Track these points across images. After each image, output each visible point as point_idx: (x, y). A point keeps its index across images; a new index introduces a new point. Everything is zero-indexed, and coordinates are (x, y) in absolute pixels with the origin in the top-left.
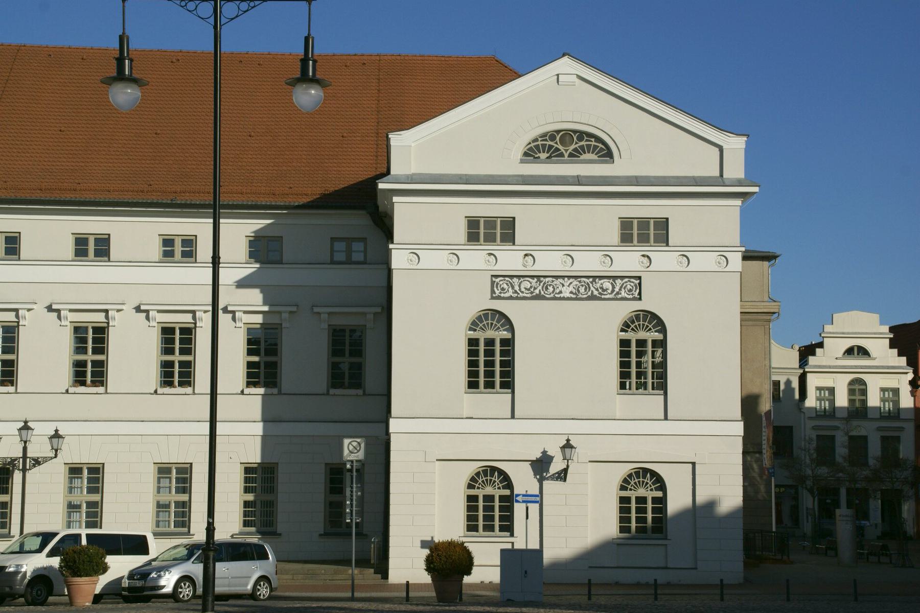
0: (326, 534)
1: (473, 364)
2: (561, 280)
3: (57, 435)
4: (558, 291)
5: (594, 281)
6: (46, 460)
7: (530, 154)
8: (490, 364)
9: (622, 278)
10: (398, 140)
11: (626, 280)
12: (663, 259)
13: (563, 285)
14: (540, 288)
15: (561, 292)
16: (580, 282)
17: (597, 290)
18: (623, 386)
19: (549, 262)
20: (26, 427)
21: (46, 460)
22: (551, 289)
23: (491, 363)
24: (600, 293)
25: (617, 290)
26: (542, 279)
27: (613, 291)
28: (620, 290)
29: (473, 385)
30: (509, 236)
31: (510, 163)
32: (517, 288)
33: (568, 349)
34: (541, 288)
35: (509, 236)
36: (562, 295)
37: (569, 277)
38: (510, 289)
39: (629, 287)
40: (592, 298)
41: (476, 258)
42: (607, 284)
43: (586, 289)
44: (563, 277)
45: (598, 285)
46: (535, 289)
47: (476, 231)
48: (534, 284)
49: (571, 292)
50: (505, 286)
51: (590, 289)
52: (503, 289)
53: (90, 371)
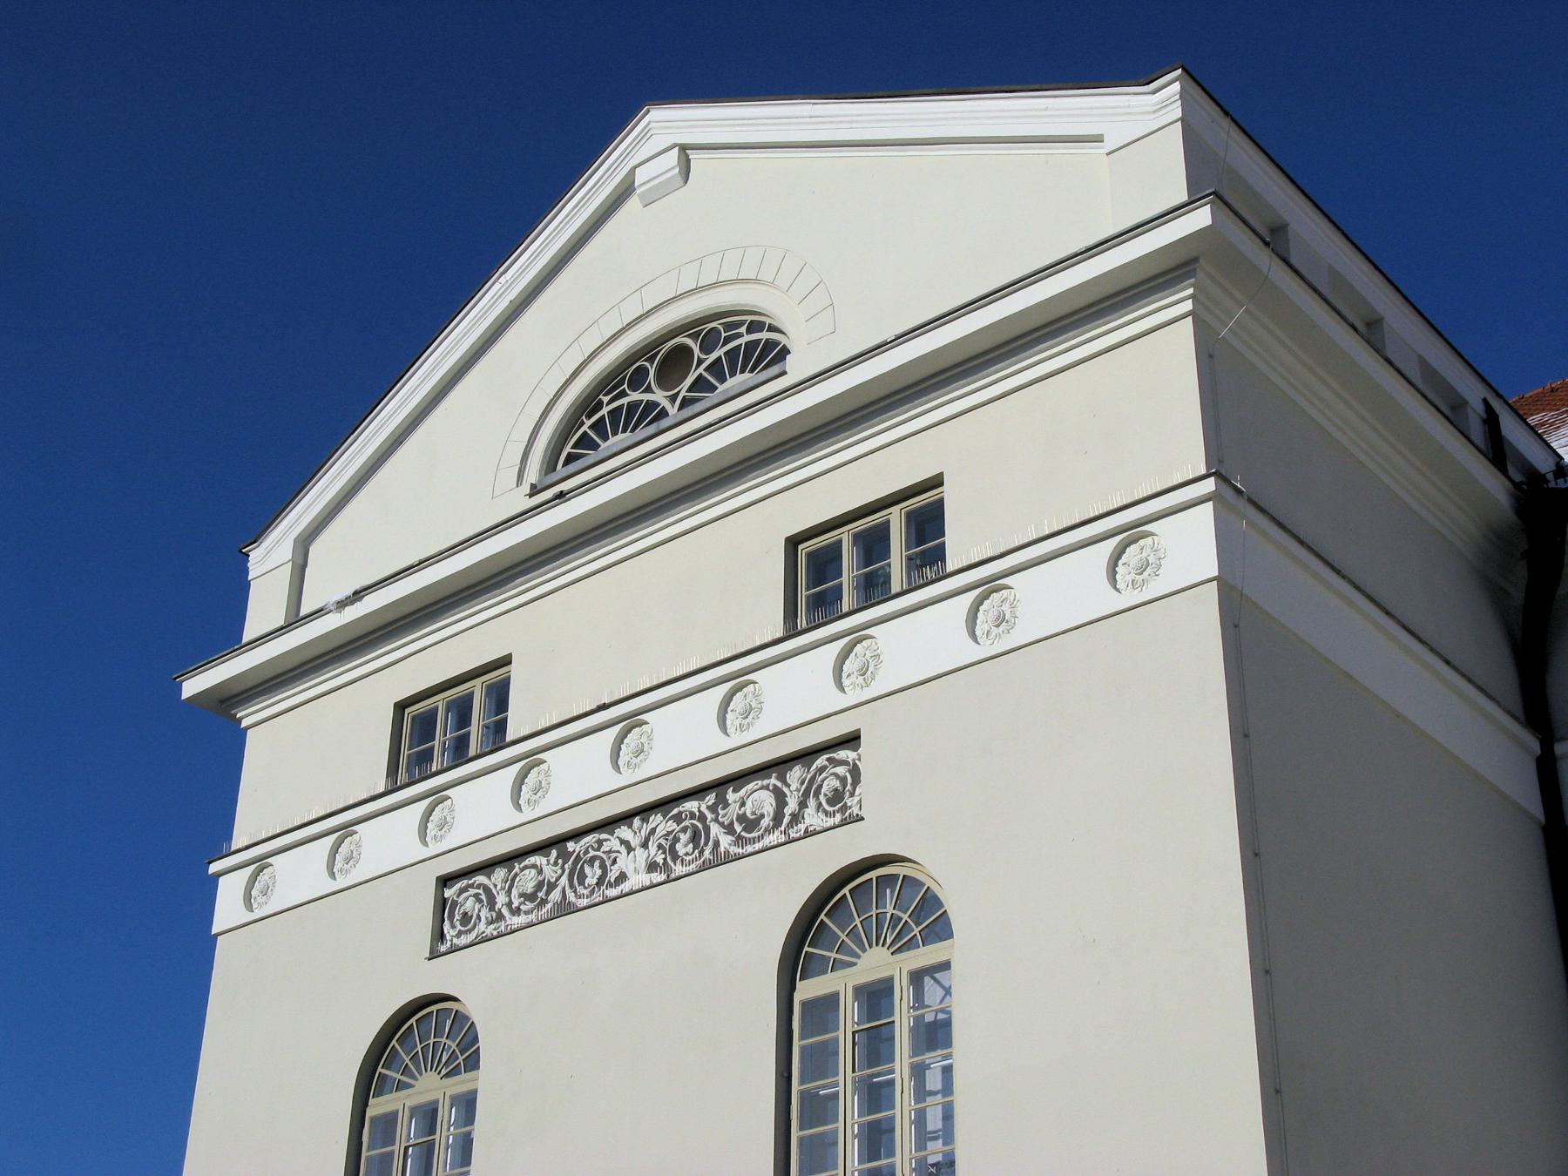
2: (624, 832)
4: (613, 875)
5: (722, 801)
9: (804, 756)
11: (821, 761)
12: (916, 637)
13: (630, 849)
14: (564, 880)
15: (622, 877)
16: (678, 819)
17: (729, 829)
22: (592, 874)
24: (739, 841)
25: (792, 805)
26: (571, 846)
27: (778, 818)
28: (803, 804)
32: (501, 899)
36: (625, 887)
37: (645, 811)
38: (484, 913)
39: (830, 784)
43: (695, 838)
44: (625, 818)
45: (733, 810)
46: (552, 886)
48: (550, 873)
49: (652, 867)
50: (469, 905)
52: (466, 918)
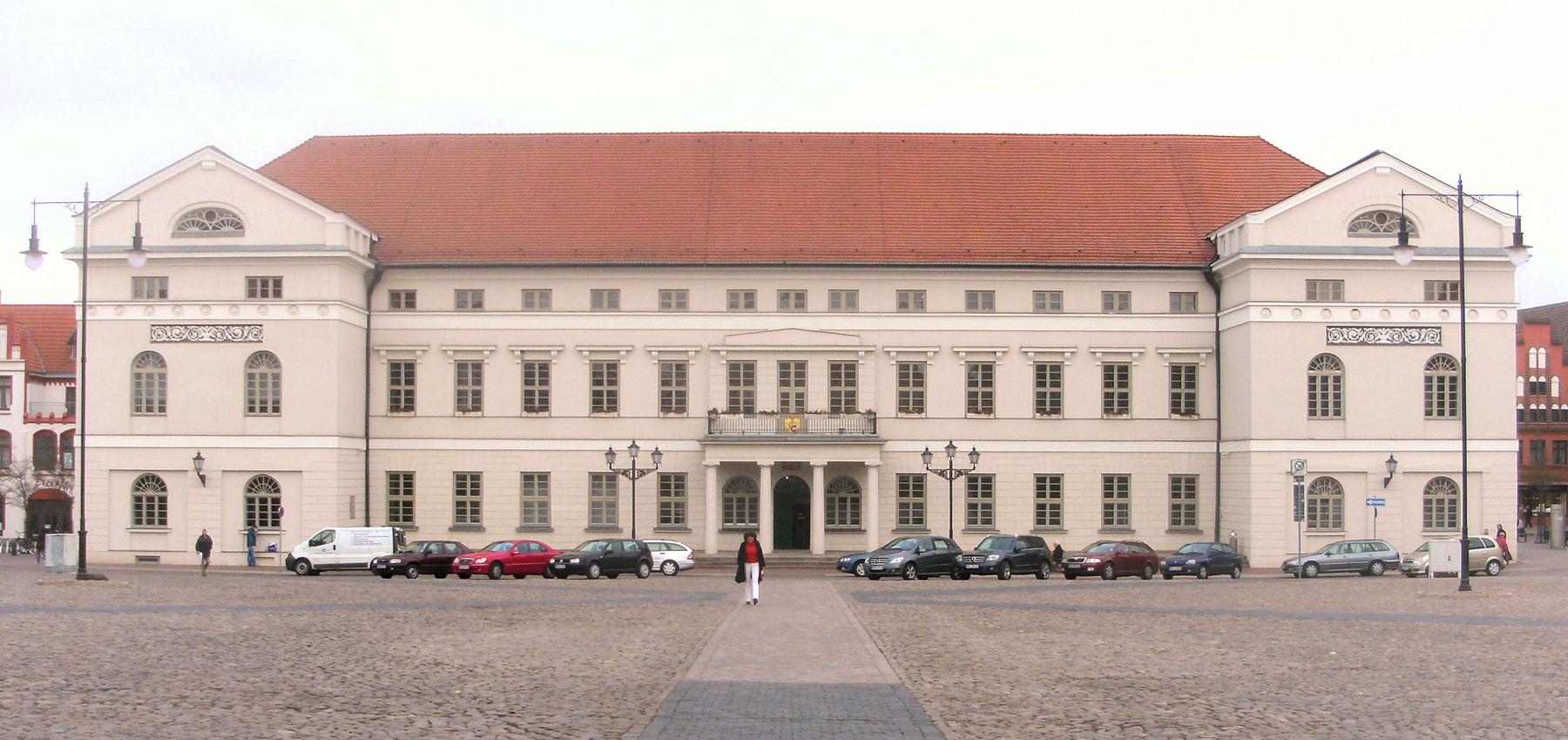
0: (1169, 531)
1: (1312, 396)
3: (657, 453)
6: (649, 471)
7: (1354, 228)
8: (1325, 396)
10: (1255, 220)
18: (1429, 413)
19: (1370, 316)
20: (634, 446)
21: (649, 471)
23: (1325, 393)
29: (1312, 413)
30: (1338, 296)
31: (1341, 238)
33: (1385, 385)
34: (1365, 336)
35: (1338, 296)
40: (1404, 344)
41: (1313, 313)
42: (1415, 333)
47: (1315, 292)
51: (1403, 336)
53: (981, 400)
